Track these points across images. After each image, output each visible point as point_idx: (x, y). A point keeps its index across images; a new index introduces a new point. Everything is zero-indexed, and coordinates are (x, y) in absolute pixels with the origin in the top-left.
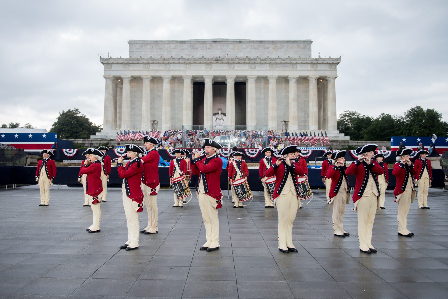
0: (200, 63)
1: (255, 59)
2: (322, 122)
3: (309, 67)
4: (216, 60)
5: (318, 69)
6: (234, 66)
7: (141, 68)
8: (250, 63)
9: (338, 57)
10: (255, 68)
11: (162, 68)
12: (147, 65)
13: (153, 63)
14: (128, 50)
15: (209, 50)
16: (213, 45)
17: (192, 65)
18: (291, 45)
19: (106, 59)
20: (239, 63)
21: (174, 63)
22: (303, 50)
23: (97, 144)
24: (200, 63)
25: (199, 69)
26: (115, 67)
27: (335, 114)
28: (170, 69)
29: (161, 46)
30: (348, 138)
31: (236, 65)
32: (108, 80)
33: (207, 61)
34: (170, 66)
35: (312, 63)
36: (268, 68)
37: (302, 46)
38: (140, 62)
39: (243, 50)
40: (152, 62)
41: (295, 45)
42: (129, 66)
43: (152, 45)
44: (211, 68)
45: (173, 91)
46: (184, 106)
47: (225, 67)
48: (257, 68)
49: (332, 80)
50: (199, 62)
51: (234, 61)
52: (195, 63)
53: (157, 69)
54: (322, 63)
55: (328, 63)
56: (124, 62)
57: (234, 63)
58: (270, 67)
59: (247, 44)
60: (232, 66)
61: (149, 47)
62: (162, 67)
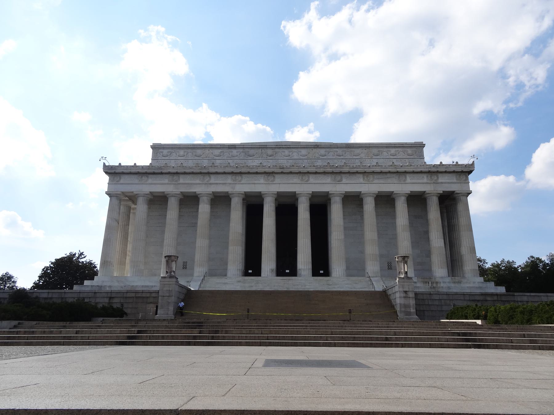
0: (257, 173)
1: (341, 167)
2: (454, 263)
3: (425, 179)
4: (280, 168)
5: (440, 181)
6: (309, 178)
8: (333, 173)
9: (471, 162)
10: (341, 180)
11: (198, 181)
12: (175, 177)
13: (185, 173)
14: (151, 158)
15: (271, 158)
16: (277, 150)
17: (244, 176)
18: (393, 151)
19: (112, 167)
20: (316, 173)
21: (217, 173)
22: (411, 157)
23: (74, 298)
24: (257, 173)
25: (256, 182)
26: (125, 179)
27: (473, 250)
29: (199, 152)
30: (502, 290)
31: (311, 176)
32: (114, 199)
33: (267, 170)
34: (210, 177)
35: (429, 172)
36: (361, 180)
37: (410, 151)
38: (164, 171)
39: (321, 157)
40: (182, 170)
41: (399, 149)
42: (148, 177)
43: (186, 150)
44: (274, 181)
45: (213, 215)
46: (230, 238)
47: (296, 179)
48: (344, 181)
49: (463, 198)
50: (254, 170)
51: (310, 170)
52: (249, 173)
53: (190, 182)
54: (446, 172)
55: (454, 172)
56: (140, 171)
57: (308, 173)
58: (364, 179)
59: (328, 150)
60: (305, 177)
61: (182, 152)
62: (197, 180)
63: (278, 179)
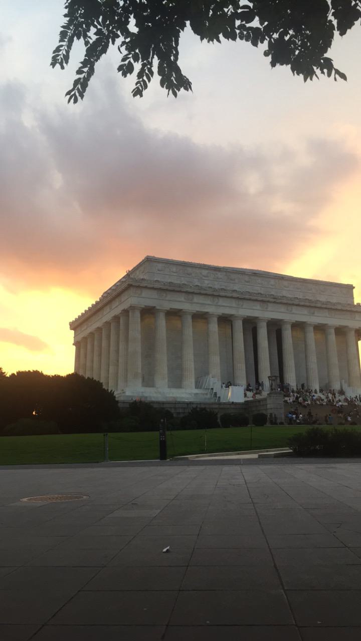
4: (274, 298)
7: (183, 299)
10: (314, 313)
11: (209, 302)
13: (200, 294)
15: (248, 284)
16: (252, 277)
21: (226, 297)
24: (256, 300)
25: (255, 308)
28: (219, 304)
29: (190, 270)
31: (294, 308)
38: (185, 290)
47: (283, 309)
52: (250, 300)
62: (208, 301)
63: (271, 307)
